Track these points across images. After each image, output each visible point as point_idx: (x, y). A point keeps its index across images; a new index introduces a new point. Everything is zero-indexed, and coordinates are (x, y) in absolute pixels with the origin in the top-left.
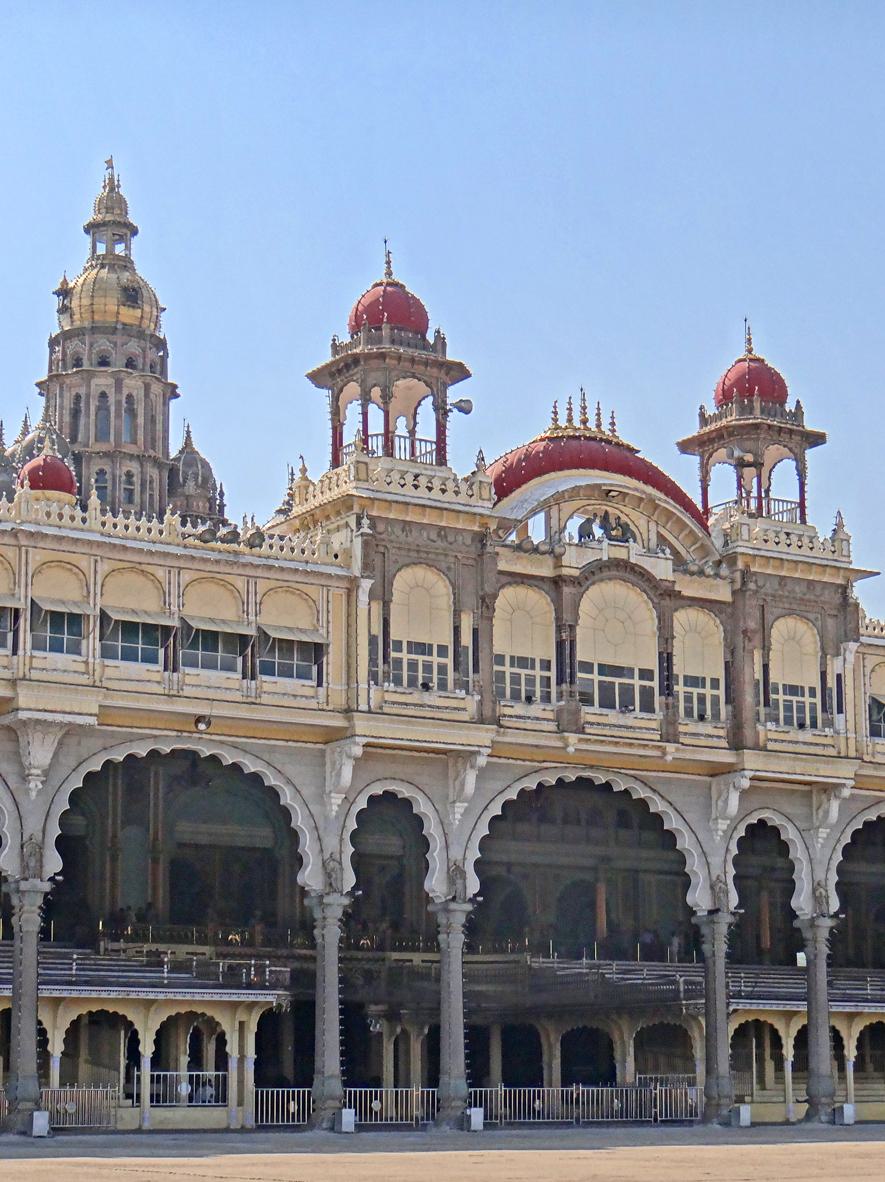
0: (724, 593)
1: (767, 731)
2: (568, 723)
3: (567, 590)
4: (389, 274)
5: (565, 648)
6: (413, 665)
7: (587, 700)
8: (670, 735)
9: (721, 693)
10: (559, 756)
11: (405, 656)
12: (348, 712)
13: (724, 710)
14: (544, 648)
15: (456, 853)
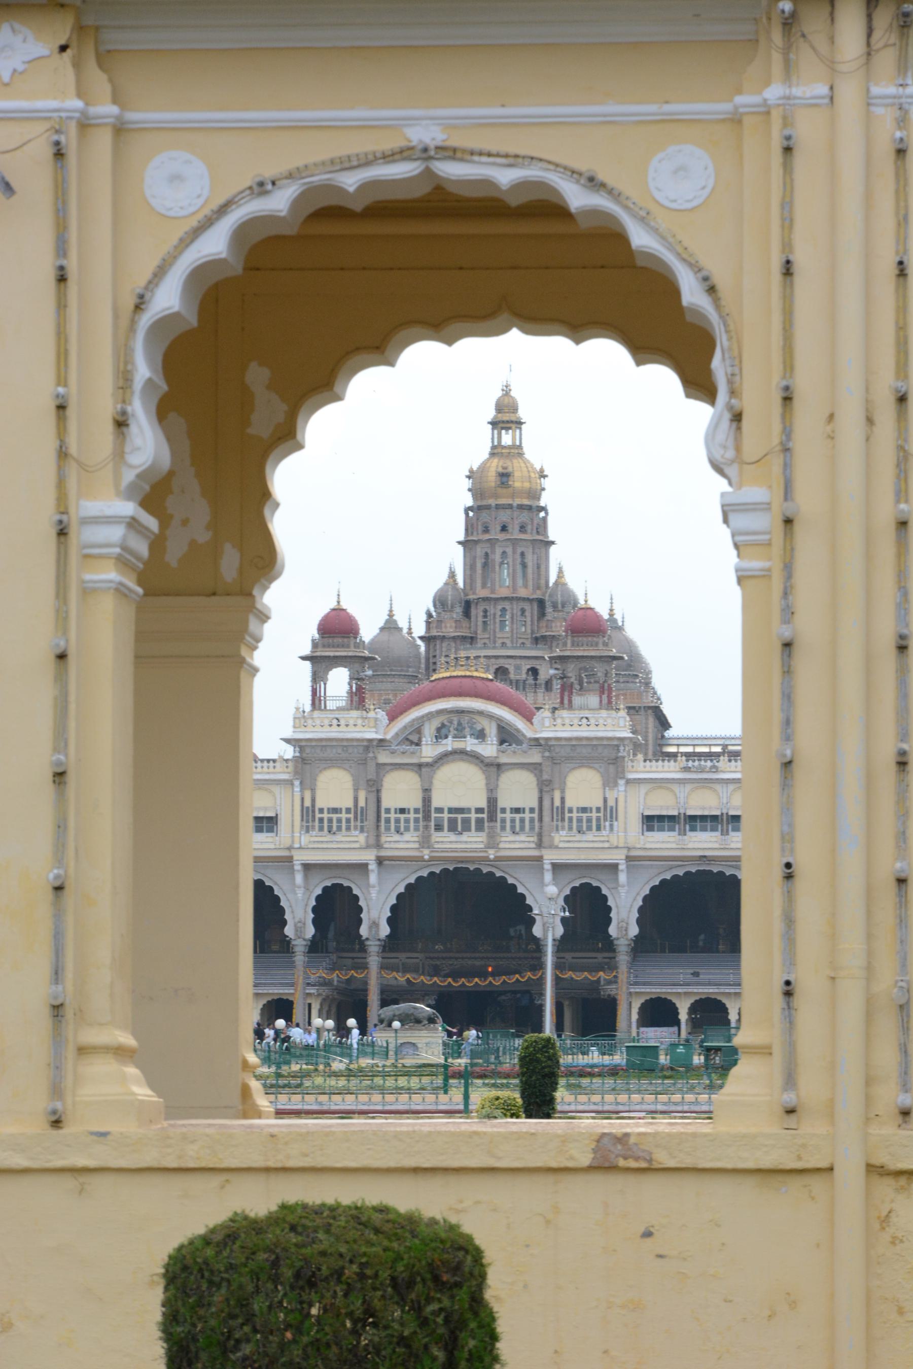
0: (535, 757)
1: (560, 837)
2: (425, 842)
3: (424, 770)
4: (339, 602)
5: (427, 801)
6: (330, 820)
7: (439, 828)
8: (492, 843)
9: (536, 815)
10: (420, 859)
11: (325, 816)
12: (289, 849)
13: (537, 824)
14: (414, 801)
15: (374, 914)
